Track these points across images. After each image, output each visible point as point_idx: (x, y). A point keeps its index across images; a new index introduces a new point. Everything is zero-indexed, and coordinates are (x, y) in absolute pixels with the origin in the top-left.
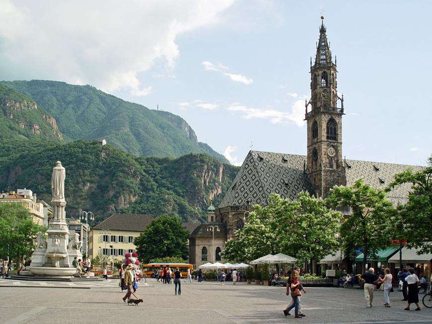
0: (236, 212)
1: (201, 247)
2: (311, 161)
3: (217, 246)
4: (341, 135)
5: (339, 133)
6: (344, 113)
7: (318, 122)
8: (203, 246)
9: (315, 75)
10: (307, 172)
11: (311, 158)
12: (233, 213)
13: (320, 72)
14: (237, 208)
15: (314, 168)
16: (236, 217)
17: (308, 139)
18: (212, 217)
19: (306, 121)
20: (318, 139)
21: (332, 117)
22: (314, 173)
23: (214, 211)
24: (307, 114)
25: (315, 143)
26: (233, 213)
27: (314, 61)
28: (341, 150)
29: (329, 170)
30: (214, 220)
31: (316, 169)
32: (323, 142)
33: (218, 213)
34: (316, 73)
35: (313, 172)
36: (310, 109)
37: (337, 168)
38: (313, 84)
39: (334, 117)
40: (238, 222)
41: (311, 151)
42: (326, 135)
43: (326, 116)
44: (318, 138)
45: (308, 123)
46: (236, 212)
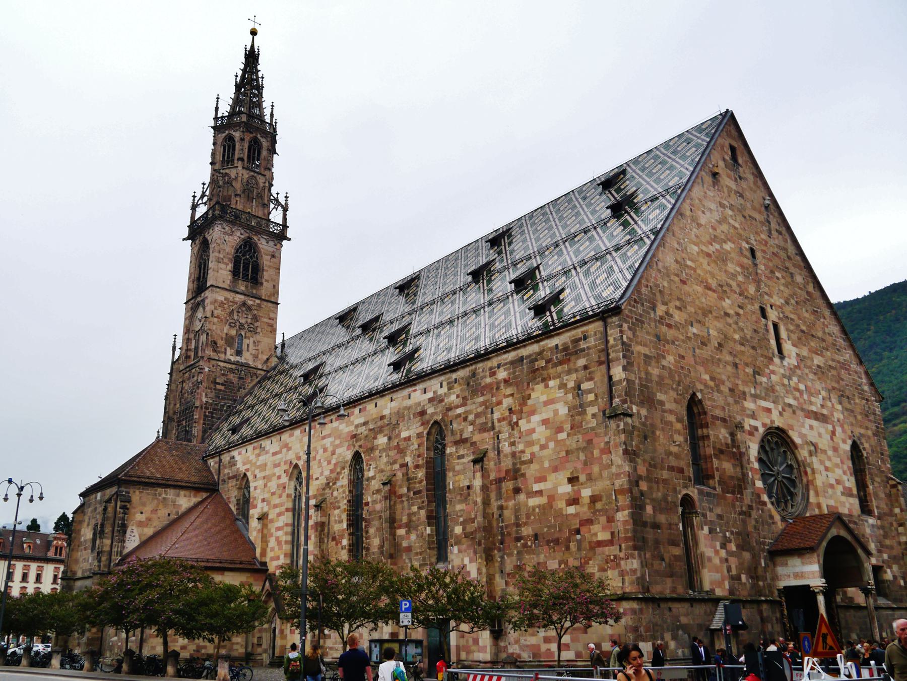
9: (230, 138)
13: (248, 137)
19: (190, 241)
27: (225, 110)
34: (237, 135)
38: (219, 158)
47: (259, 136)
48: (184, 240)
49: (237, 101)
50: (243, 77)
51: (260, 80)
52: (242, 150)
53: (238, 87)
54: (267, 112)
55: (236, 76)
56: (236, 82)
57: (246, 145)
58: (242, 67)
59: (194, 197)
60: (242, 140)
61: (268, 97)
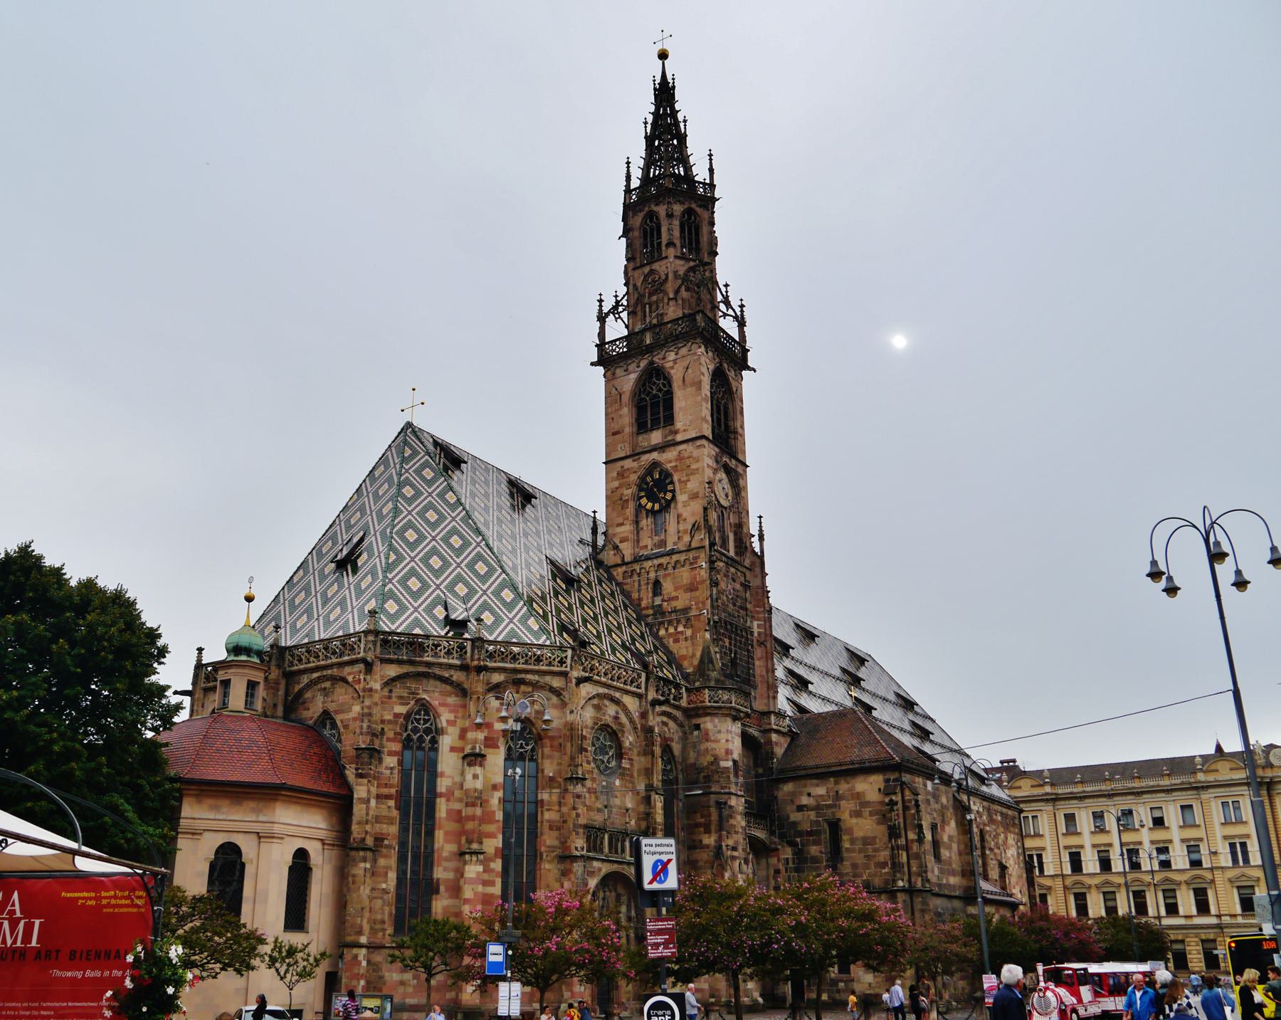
0: (406, 669)
1: (210, 844)
2: (631, 518)
3: (299, 844)
4: (743, 436)
5: (740, 430)
6: (750, 364)
7: (676, 374)
8: (221, 839)
9: (652, 216)
10: (609, 557)
11: (632, 505)
12: (392, 671)
13: (678, 209)
14: (415, 644)
15: (647, 541)
16: (399, 690)
17: (612, 433)
18: (252, 685)
19: (601, 370)
20: (676, 432)
21: (721, 365)
22: (648, 564)
23: (259, 653)
24: (601, 346)
25: (661, 448)
26: (392, 671)
27: (637, 174)
28: (745, 488)
29: (724, 554)
30: (259, 705)
31: (663, 543)
32: (704, 442)
33: (274, 674)
34: (661, 210)
35: (637, 559)
36: (617, 329)
37: (736, 553)
39: (725, 365)
40: (407, 716)
41: (634, 478)
42: (709, 418)
43: (710, 354)
44: (679, 425)
45: (610, 379)
46: (406, 669)
47: (694, 206)
48: (592, 364)
49: (649, 162)
50: (654, 124)
51: (682, 125)
52: (670, 230)
53: (649, 140)
54: (700, 173)
55: (646, 123)
56: (646, 133)
57: (676, 223)
58: (652, 108)
59: (601, 301)
60: (670, 216)
61: (696, 150)
